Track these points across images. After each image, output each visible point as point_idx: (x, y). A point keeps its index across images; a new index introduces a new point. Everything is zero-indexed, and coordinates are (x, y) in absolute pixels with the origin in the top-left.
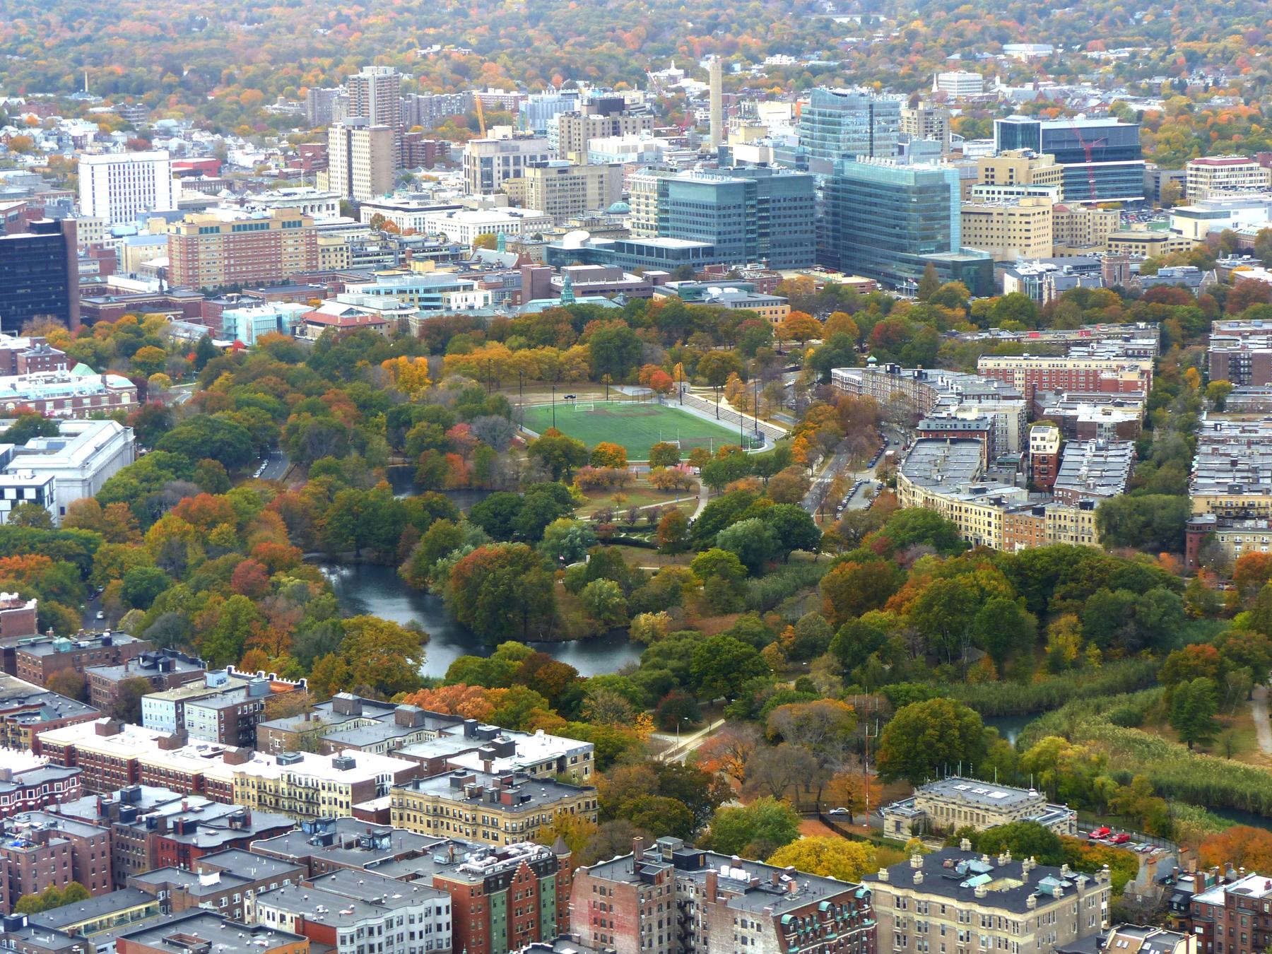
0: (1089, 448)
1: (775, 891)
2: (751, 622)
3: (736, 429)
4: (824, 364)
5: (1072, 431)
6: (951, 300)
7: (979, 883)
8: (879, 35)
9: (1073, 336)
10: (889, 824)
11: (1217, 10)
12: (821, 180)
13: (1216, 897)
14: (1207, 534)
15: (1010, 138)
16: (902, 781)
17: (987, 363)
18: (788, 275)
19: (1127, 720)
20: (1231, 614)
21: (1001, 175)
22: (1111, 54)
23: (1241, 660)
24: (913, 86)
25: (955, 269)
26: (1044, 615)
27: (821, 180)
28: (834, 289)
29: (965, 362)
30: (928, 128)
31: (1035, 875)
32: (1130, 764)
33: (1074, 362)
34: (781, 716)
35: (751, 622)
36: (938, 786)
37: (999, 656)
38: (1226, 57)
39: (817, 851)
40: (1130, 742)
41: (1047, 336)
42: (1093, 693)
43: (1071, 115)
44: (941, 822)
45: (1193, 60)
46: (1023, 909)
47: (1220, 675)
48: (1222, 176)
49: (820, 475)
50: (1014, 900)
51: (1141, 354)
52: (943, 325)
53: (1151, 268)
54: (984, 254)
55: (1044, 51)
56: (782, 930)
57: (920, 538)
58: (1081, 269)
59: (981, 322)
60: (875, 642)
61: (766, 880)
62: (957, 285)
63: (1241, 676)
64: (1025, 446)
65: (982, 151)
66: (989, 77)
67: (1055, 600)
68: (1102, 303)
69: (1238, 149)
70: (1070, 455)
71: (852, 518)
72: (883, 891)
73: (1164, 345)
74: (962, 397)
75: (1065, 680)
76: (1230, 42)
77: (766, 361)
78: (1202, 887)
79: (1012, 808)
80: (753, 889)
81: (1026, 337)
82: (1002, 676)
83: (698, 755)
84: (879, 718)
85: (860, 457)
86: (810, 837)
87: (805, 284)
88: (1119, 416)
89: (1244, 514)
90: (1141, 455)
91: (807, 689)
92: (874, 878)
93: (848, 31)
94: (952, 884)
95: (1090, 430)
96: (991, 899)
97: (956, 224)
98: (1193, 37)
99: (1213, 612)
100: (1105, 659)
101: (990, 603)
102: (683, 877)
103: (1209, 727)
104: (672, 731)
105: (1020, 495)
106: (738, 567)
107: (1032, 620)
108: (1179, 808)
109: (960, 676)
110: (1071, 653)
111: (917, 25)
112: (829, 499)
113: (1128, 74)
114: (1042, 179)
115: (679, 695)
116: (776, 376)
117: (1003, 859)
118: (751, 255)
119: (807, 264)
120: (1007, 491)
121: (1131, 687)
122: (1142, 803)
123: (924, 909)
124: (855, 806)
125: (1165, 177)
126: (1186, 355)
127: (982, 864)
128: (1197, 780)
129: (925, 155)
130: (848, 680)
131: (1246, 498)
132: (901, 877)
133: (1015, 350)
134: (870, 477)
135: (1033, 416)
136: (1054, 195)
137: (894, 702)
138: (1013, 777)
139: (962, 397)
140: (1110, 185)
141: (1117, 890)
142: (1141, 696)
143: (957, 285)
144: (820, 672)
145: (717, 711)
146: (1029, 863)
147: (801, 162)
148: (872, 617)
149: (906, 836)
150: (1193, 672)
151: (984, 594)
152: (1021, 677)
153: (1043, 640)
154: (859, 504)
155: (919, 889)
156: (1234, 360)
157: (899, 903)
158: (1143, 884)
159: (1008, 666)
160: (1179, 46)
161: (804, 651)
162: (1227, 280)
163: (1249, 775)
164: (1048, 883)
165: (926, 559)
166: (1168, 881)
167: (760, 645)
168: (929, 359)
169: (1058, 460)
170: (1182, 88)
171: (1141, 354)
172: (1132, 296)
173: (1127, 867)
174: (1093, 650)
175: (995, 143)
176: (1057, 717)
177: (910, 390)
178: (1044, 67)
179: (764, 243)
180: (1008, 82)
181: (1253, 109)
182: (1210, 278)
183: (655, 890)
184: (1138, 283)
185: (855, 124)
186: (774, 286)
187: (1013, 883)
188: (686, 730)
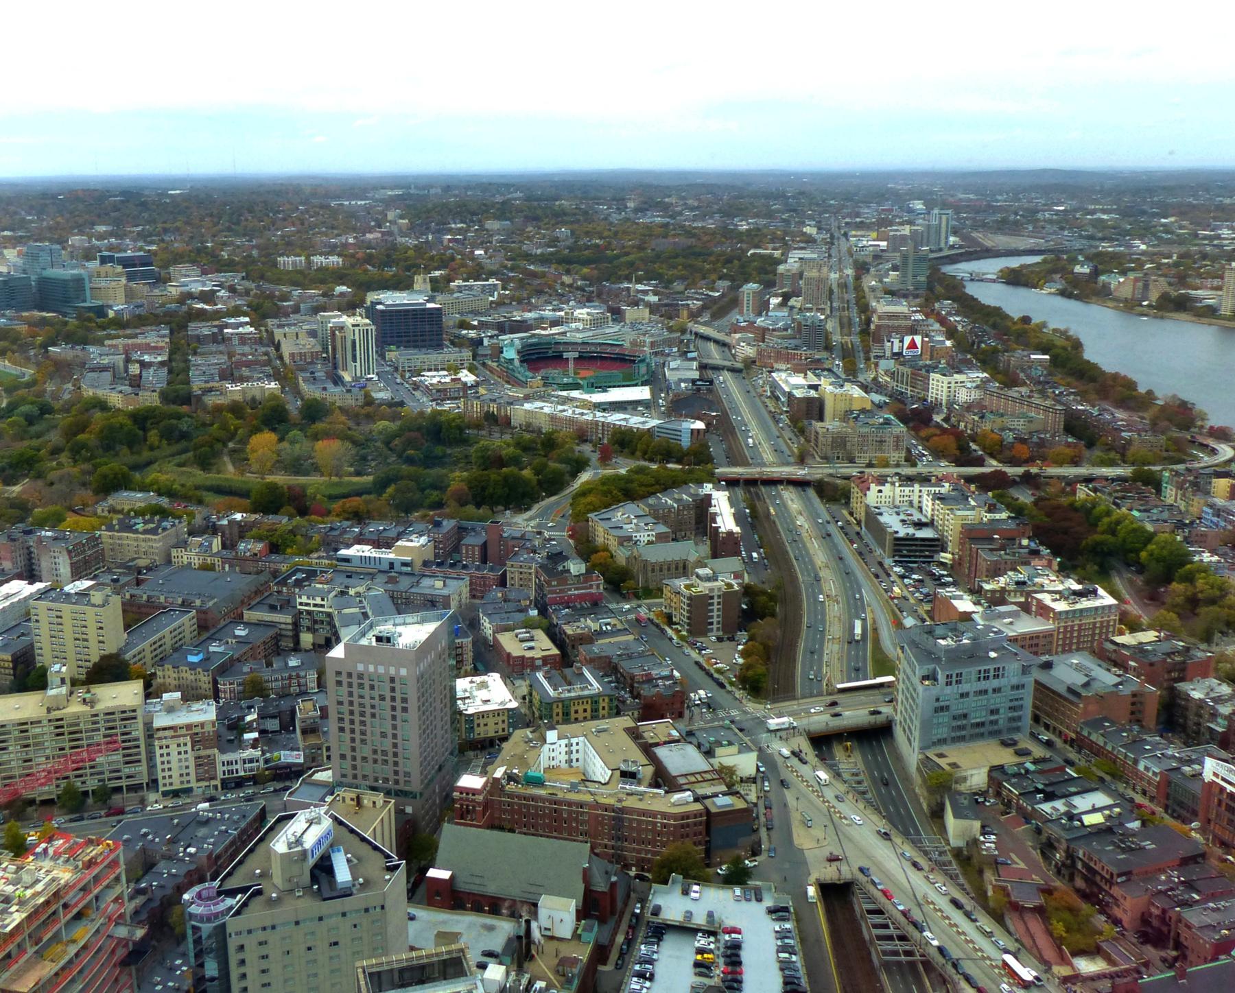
0: (151, 370)
1: (64, 539)
2: (35, 443)
3: (14, 372)
4: (45, 346)
5: (143, 365)
6: (90, 320)
7: (140, 527)
8: (45, 224)
9: (138, 331)
10: (99, 510)
11: (172, 213)
12: (33, 277)
13: (225, 522)
14: (199, 398)
15: (104, 260)
16: (101, 495)
17: (107, 342)
18: (24, 314)
19: (180, 465)
20: (212, 425)
21: (103, 274)
22: (135, 229)
23: (218, 440)
24: (62, 242)
25: (90, 309)
26: (144, 429)
27: (33, 277)
28: (44, 318)
29: (99, 342)
30: (72, 258)
31: (160, 522)
32: (183, 480)
33: (140, 340)
34: (53, 476)
35: (35, 443)
36: (116, 495)
37: (130, 447)
38: (178, 229)
39: (77, 523)
40: (183, 473)
41: (128, 332)
42: (166, 457)
43: (125, 251)
44: (119, 508)
45: (165, 231)
46: (157, 534)
47: (211, 446)
48: (183, 272)
49: (50, 387)
50: (153, 532)
51: (164, 336)
52: (89, 329)
53: (163, 305)
54: (100, 303)
55: (110, 228)
56: (69, 552)
57: (94, 407)
58: (137, 307)
59: (103, 328)
60: (84, 446)
61: (60, 535)
62: (91, 315)
63: (219, 446)
64: (126, 370)
65: (94, 265)
66: (90, 239)
67: (148, 425)
68: (146, 319)
69: (187, 262)
70: (144, 374)
71: (66, 402)
72: (104, 534)
73: (172, 332)
74: (101, 355)
75: (156, 453)
76: (178, 224)
77: (21, 346)
78: (219, 519)
79: (145, 500)
80: (55, 539)
81: (121, 332)
82: (132, 453)
83: (23, 492)
84: (89, 473)
85: (66, 378)
86: (71, 519)
87: (32, 317)
88: (159, 359)
89: (211, 390)
90: (170, 372)
91: (60, 465)
92: (100, 530)
93: (32, 221)
94: (129, 528)
95: (150, 364)
96: (146, 532)
97: (88, 293)
98: (165, 222)
99: (204, 425)
100: (169, 444)
101: (126, 429)
102: (27, 538)
103: (210, 464)
104: (9, 485)
105: (128, 389)
106: (25, 423)
107: (141, 433)
108: (204, 493)
109: (117, 455)
110: (156, 443)
111: (59, 219)
112: (55, 396)
113: (141, 236)
114: (118, 275)
115: (10, 472)
116: (26, 352)
117: (147, 517)
118: (9, 307)
119: (28, 310)
120: (123, 388)
121: (180, 453)
122: (191, 493)
123: (120, 538)
124: (85, 505)
125: (163, 273)
126: (181, 335)
127: (140, 520)
128: (208, 483)
129: (73, 268)
130: (75, 461)
131: (211, 384)
132: (110, 528)
133: (118, 337)
134: (70, 386)
135: (128, 360)
136: (124, 280)
137: (96, 467)
138: (143, 488)
139: (101, 355)
140: (144, 276)
141: (189, 524)
142: (184, 456)
143: (91, 315)
144: (64, 458)
145: (26, 476)
146: (157, 517)
147: (24, 271)
148: (80, 437)
149: (106, 514)
150: (202, 446)
151: (122, 426)
152: (139, 453)
153: (145, 440)
154: (67, 397)
155: (118, 531)
156: (198, 337)
157: (110, 537)
158: (198, 520)
159: (135, 450)
160: (159, 225)
161: (56, 451)
162: (191, 309)
163: (227, 480)
164: (164, 524)
165: (98, 415)
166: (207, 519)
167: (39, 450)
168: (85, 342)
169: (140, 376)
170: (163, 241)
171: (164, 336)
172: (156, 316)
173: (191, 515)
174: (164, 442)
175: (98, 262)
176: (155, 466)
177: (80, 353)
178: (111, 234)
179: (13, 302)
180: (97, 240)
181: (190, 248)
182: (185, 308)
183: (17, 543)
184: (159, 311)
185: (45, 258)
186: (21, 318)
187: (152, 526)
188: (15, 484)
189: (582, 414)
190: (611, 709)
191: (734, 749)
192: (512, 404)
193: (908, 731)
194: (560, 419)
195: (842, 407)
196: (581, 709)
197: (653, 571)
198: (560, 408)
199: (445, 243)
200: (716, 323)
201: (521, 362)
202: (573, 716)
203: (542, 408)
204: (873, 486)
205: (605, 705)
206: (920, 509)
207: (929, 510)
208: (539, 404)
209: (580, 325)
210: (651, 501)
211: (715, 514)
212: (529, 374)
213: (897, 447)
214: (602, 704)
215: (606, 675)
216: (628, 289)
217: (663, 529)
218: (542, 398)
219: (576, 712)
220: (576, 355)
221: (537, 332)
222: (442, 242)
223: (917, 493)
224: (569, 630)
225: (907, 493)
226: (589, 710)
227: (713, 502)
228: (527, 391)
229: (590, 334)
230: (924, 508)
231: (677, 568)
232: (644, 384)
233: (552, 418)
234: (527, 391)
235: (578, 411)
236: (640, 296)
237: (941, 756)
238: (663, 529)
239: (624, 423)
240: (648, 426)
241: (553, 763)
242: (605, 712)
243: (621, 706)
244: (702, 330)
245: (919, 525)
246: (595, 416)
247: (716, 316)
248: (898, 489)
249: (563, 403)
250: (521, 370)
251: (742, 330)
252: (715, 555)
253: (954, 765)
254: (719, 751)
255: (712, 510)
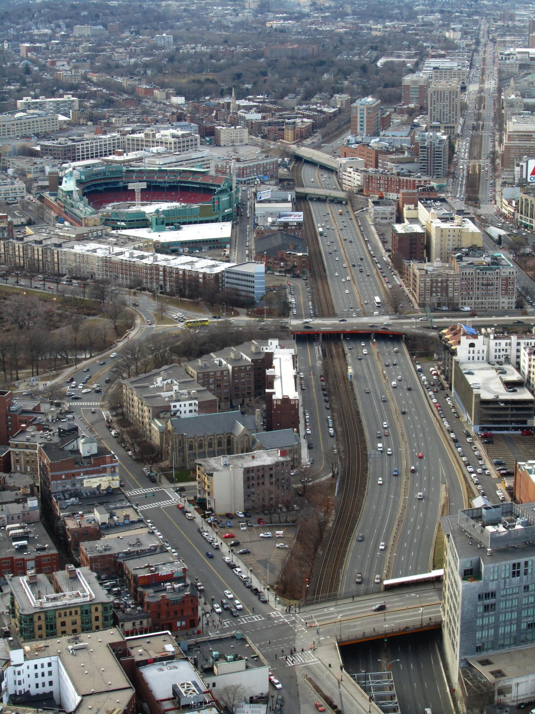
189: (142, 257)
190: (106, 619)
191: (241, 664)
192: (60, 246)
193: (452, 633)
194: (115, 263)
195: (450, 245)
196: (68, 620)
197: (191, 448)
198: (117, 249)
199: (23, 53)
200: (328, 146)
201: (84, 194)
202: (59, 628)
203: (95, 251)
204: (463, 339)
205: (99, 614)
206: (518, 369)
207: (526, 367)
208: (92, 245)
209: (161, 149)
210: (200, 362)
211: (273, 377)
212: (89, 210)
213: (506, 292)
214: (94, 614)
215: (109, 578)
216: (229, 104)
217: (210, 396)
218: (98, 238)
219: (63, 624)
220: (144, 185)
221: (110, 158)
222: (18, 51)
223: (514, 346)
224: (71, 524)
225: (503, 346)
226: (79, 622)
227: (275, 363)
228: (83, 230)
229: (173, 159)
230: (522, 363)
231: (220, 444)
232: (225, 219)
233: (106, 261)
234: (83, 230)
235: (137, 253)
236: (240, 113)
237: (485, 662)
238: (210, 396)
239: (188, 268)
240: (217, 270)
241: (19, 688)
242: (99, 623)
243: (119, 614)
244: (305, 152)
245: (511, 385)
246: (156, 259)
247: (329, 137)
248: (493, 343)
249: (123, 244)
250: (81, 205)
251: (353, 153)
252: (269, 426)
253: (498, 674)
254: (221, 667)
255: (269, 372)
